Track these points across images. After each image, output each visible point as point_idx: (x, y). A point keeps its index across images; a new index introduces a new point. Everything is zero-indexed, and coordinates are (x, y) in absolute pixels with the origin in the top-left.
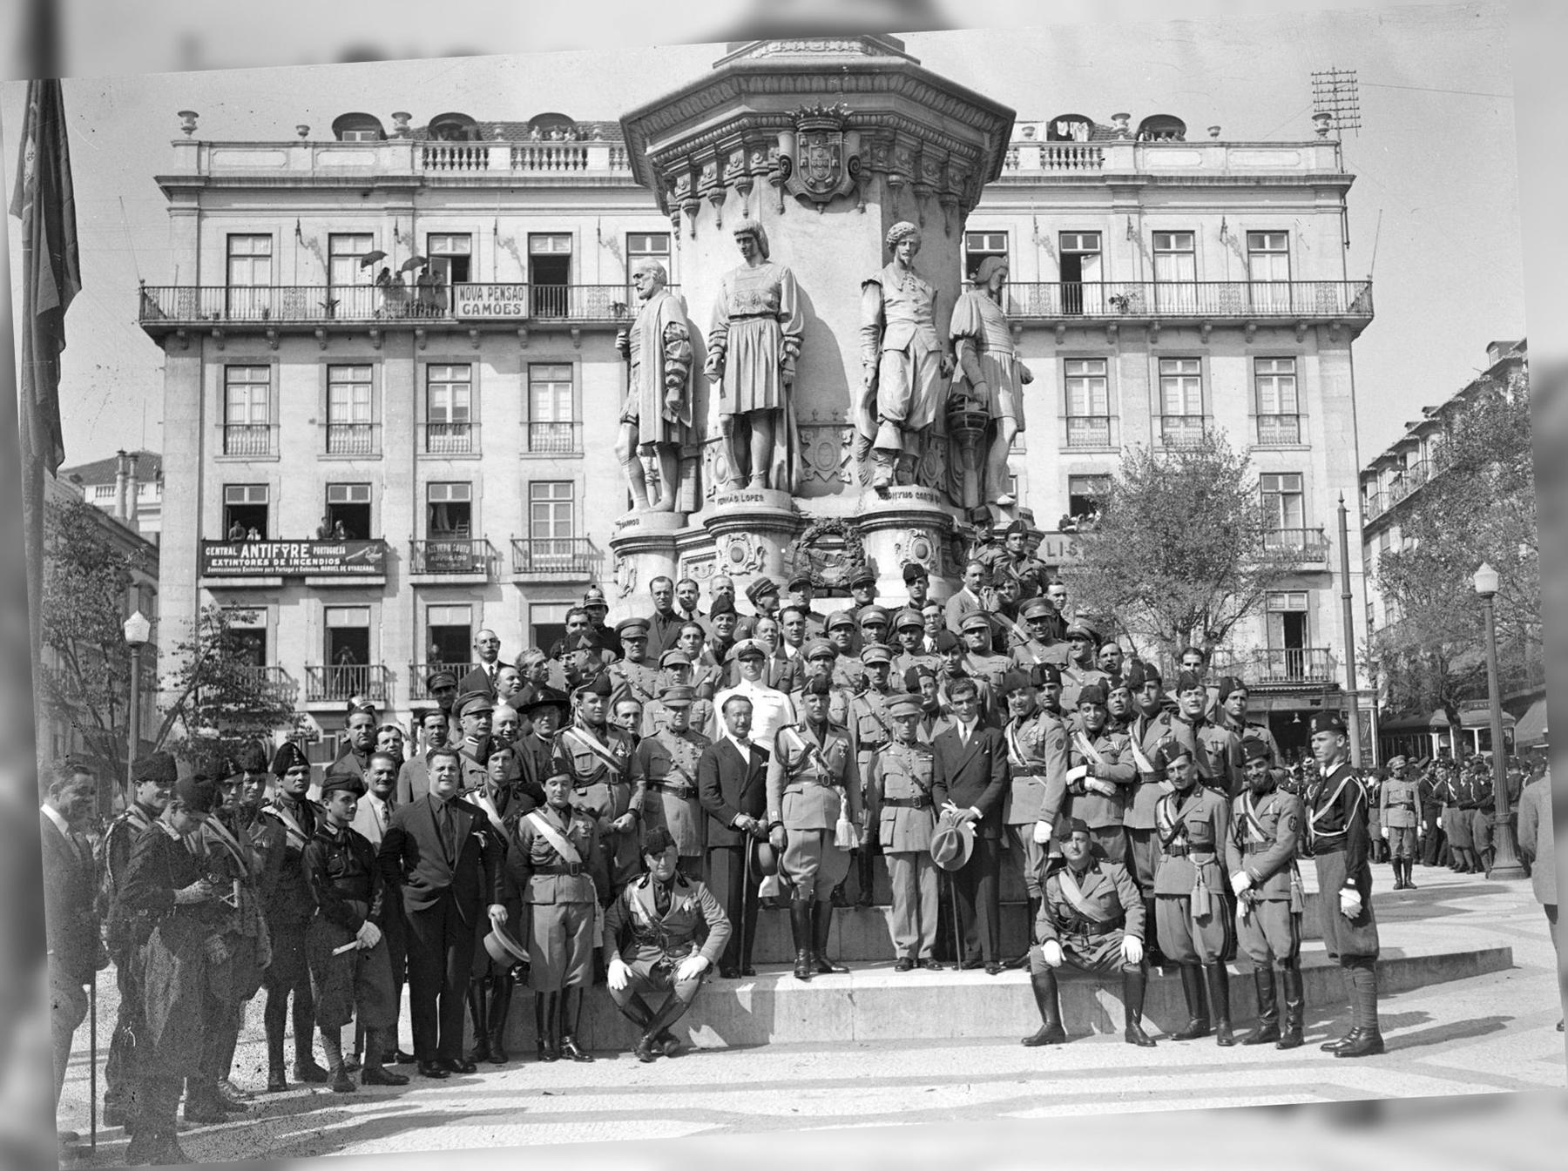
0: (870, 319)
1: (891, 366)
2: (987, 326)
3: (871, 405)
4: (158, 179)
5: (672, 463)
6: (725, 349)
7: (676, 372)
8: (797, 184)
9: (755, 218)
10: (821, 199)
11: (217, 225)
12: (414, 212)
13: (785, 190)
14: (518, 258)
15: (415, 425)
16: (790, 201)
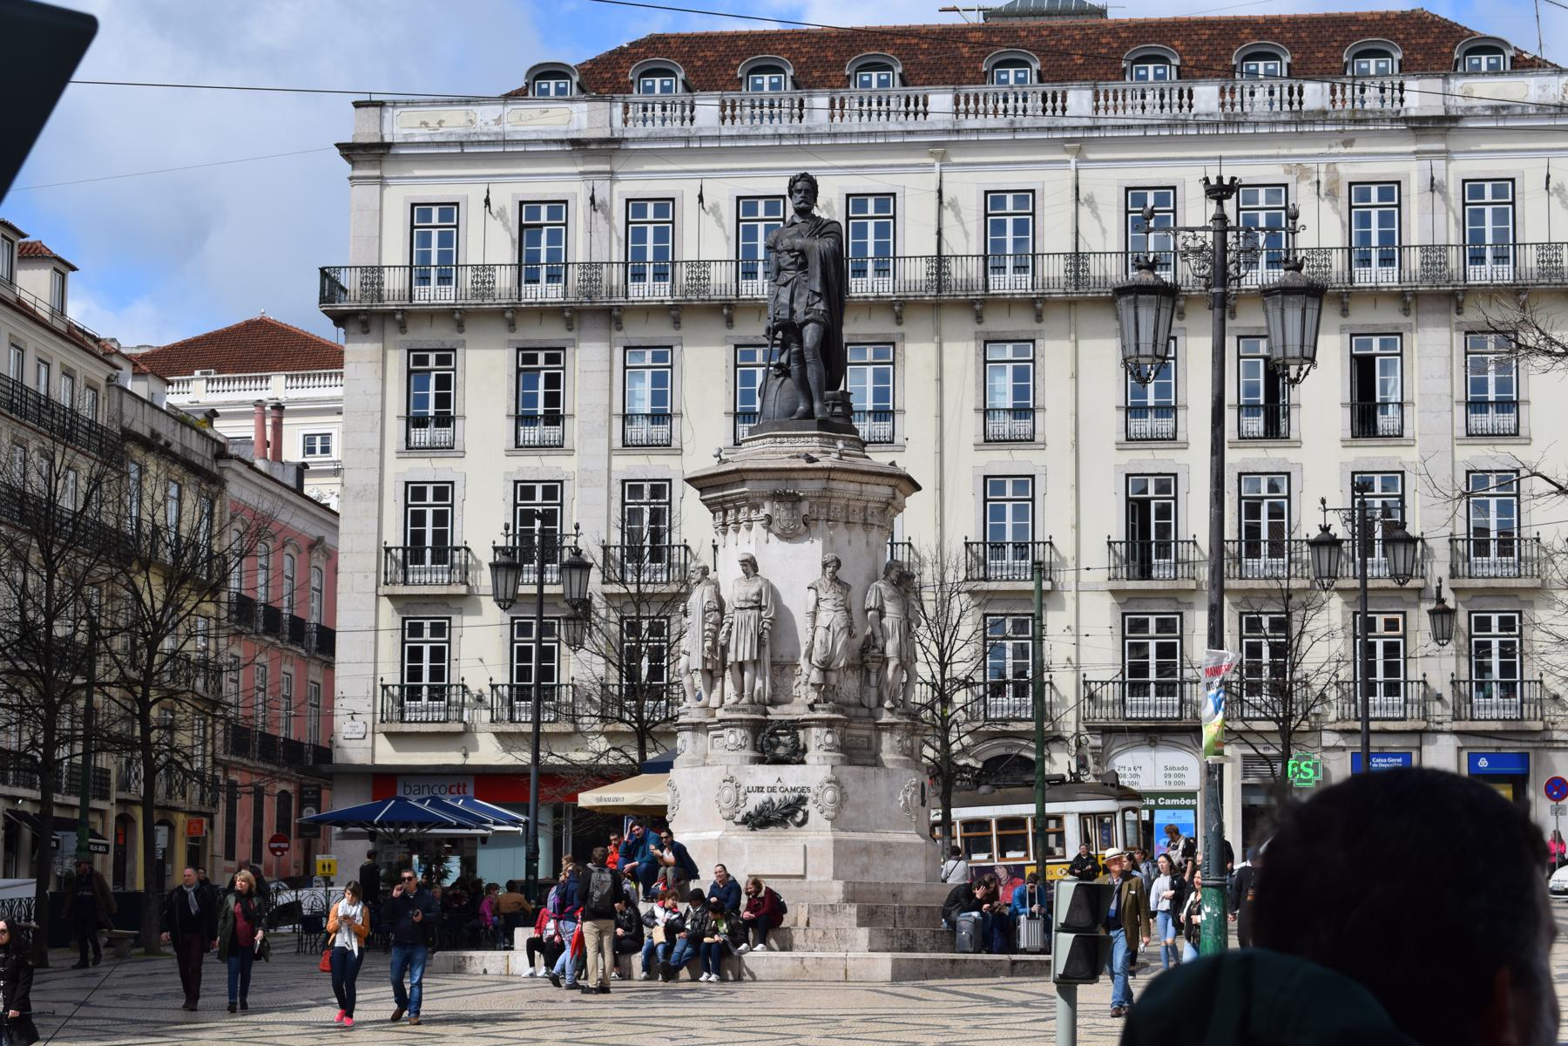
0: (811, 609)
1: (820, 633)
2: (886, 603)
3: (809, 655)
4: (337, 145)
5: (708, 679)
8: (776, 527)
10: (787, 536)
11: (399, 196)
12: (612, 176)
13: (769, 531)
14: (722, 226)
15: (610, 415)
16: (772, 536)
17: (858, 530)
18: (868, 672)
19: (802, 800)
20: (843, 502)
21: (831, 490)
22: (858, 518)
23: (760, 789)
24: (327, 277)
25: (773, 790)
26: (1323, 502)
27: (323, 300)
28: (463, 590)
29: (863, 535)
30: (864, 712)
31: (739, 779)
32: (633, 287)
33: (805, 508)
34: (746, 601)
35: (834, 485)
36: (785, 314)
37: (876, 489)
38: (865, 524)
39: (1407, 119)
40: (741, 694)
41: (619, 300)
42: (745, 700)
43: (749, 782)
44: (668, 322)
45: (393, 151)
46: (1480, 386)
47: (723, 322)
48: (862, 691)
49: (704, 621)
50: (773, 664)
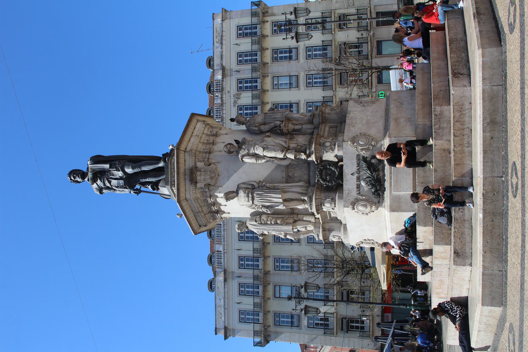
4: (225, 339)
6: (263, 206)
7: (271, 221)
9: (222, 195)
17: (218, 140)
18: (294, 130)
19: (365, 159)
20: (200, 145)
21: (191, 150)
22: (212, 139)
23: (359, 187)
24: (256, 344)
25: (358, 179)
26: (284, 39)
27: (262, 346)
28: (335, 314)
29: (222, 137)
30: (316, 132)
31: (352, 199)
32: (260, 267)
33: (200, 165)
34: (248, 196)
35: (188, 149)
36: (122, 182)
37: (196, 129)
38: (216, 135)
39: (223, 78)
40: (304, 201)
41: (262, 271)
42: (306, 198)
43: (354, 193)
44: (268, 259)
45: (226, 326)
46: (286, 58)
47: (269, 245)
48: (304, 134)
49: (266, 224)
50: (287, 182)
